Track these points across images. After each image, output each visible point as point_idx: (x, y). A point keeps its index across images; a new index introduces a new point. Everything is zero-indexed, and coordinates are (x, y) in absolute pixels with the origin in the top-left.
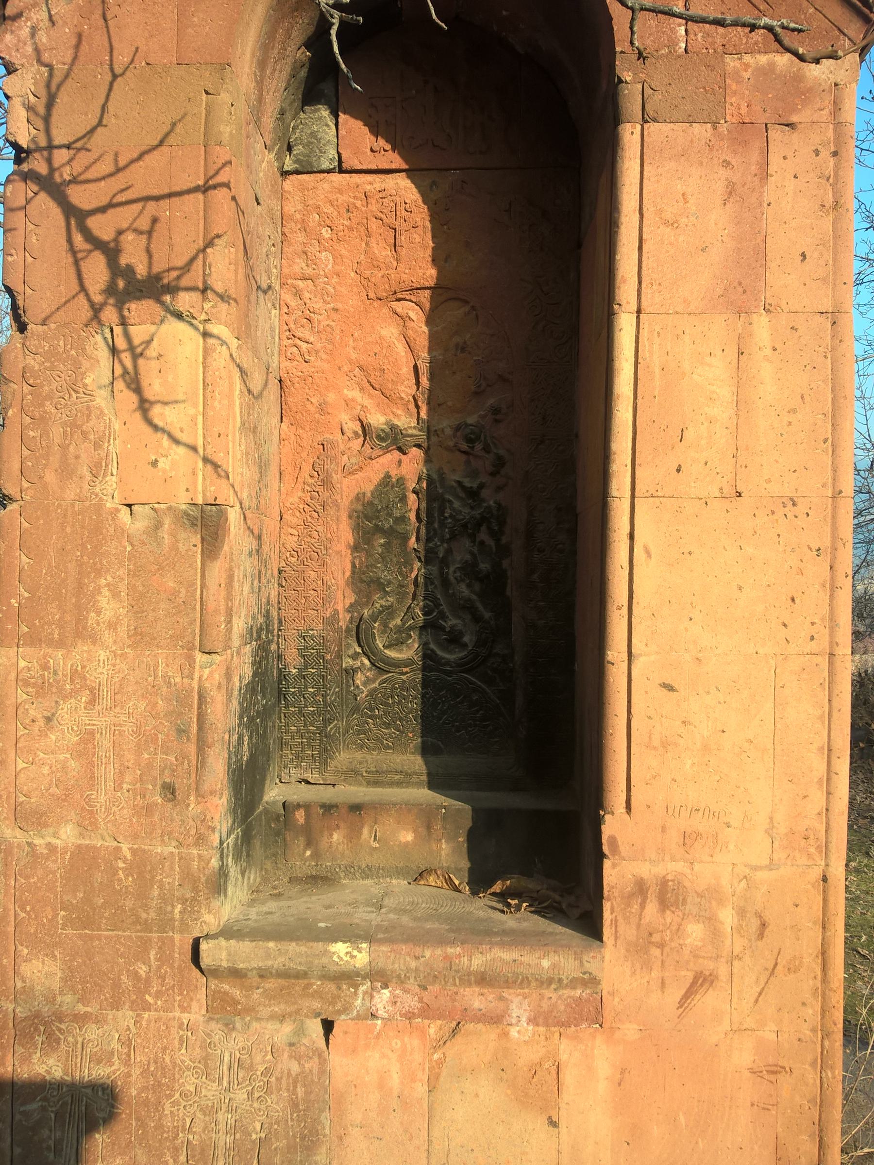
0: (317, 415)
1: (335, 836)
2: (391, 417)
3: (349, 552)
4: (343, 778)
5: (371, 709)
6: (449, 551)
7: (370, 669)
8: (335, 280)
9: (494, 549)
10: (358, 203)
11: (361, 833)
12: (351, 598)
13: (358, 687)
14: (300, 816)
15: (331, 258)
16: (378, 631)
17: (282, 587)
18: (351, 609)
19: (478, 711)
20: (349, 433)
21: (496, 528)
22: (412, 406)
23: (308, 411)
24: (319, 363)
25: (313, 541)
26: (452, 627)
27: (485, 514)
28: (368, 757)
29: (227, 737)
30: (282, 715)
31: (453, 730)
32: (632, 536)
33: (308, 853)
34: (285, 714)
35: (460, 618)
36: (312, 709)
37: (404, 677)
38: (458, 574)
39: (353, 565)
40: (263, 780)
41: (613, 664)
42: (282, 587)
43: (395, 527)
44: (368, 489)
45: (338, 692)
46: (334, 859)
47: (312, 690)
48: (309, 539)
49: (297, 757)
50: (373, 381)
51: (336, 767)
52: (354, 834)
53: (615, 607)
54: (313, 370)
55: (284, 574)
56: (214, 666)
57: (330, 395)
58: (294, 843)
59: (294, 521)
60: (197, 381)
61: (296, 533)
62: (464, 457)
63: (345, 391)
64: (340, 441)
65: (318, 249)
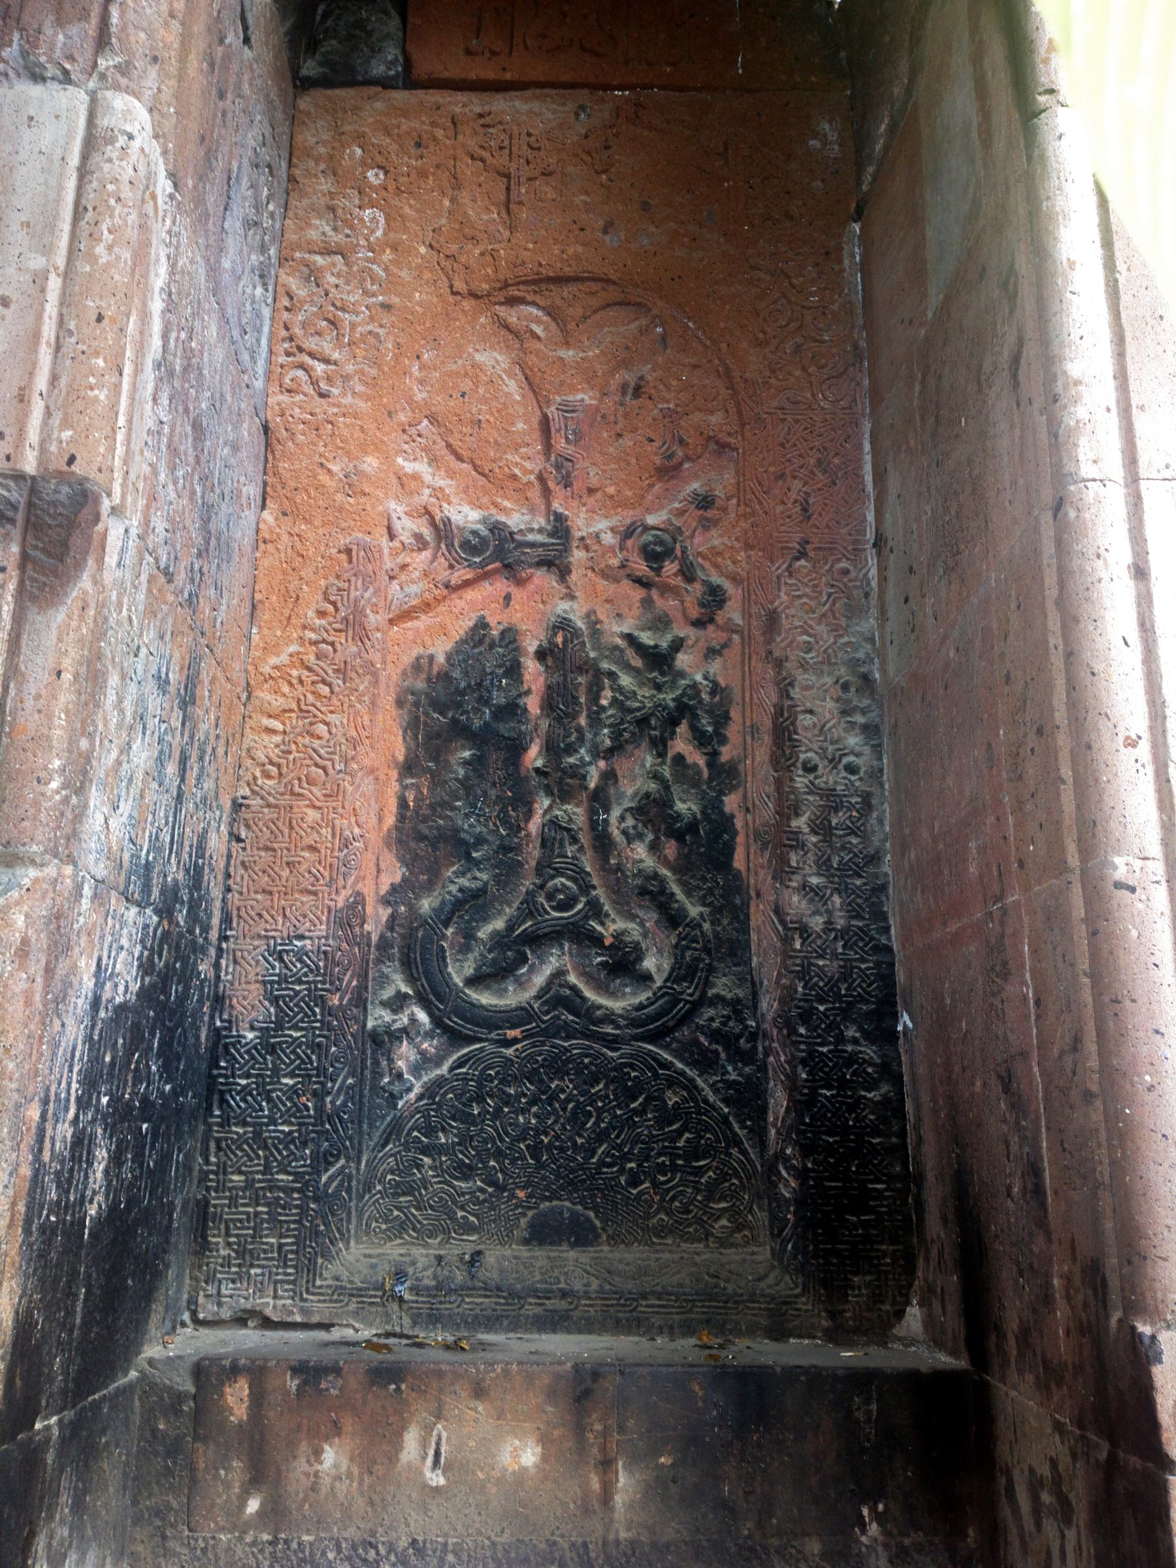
0: (339, 497)
1: (330, 1456)
2: (493, 511)
3: (394, 774)
4: (353, 1306)
5: (430, 1131)
6: (609, 776)
7: (429, 1035)
8: (388, 255)
9: (706, 773)
10: (439, 133)
11: (398, 1446)
12: (394, 873)
13: (400, 1076)
14: (236, 1398)
15: (382, 220)
16: (452, 946)
17: (239, 840)
18: (394, 896)
19: (680, 1133)
20: (406, 538)
21: (710, 729)
22: (535, 494)
23: (320, 487)
24: (349, 400)
25: (316, 743)
26: (618, 936)
27: (685, 700)
28: (418, 1252)
29: (34, 1113)
30: (213, 1146)
31: (623, 1180)
32: (1140, 572)
33: (253, 1505)
34: (218, 1141)
35: (632, 917)
36: (287, 1129)
37: (509, 1052)
38: (630, 822)
39: (403, 803)
40: (147, 1295)
41: (1133, 890)
42: (239, 840)
43: (494, 725)
44: (440, 649)
45: (351, 1087)
46: (321, 1522)
47: (290, 1082)
48: (307, 740)
49: (241, 1254)
50: (456, 444)
51: (337, 1279)
52: (380, 1442)
53: (1120, 739)
54: (335, 410)
55: (244, 814)
56: (15, 894)
57: (369, 459)
58: (216, 1477)
59: (278, 703)
60: (58, 201)
61: (280, 727)
62: (638, 594)
63: (400, 460)
64: (386, 551)
65: (357, 202)
